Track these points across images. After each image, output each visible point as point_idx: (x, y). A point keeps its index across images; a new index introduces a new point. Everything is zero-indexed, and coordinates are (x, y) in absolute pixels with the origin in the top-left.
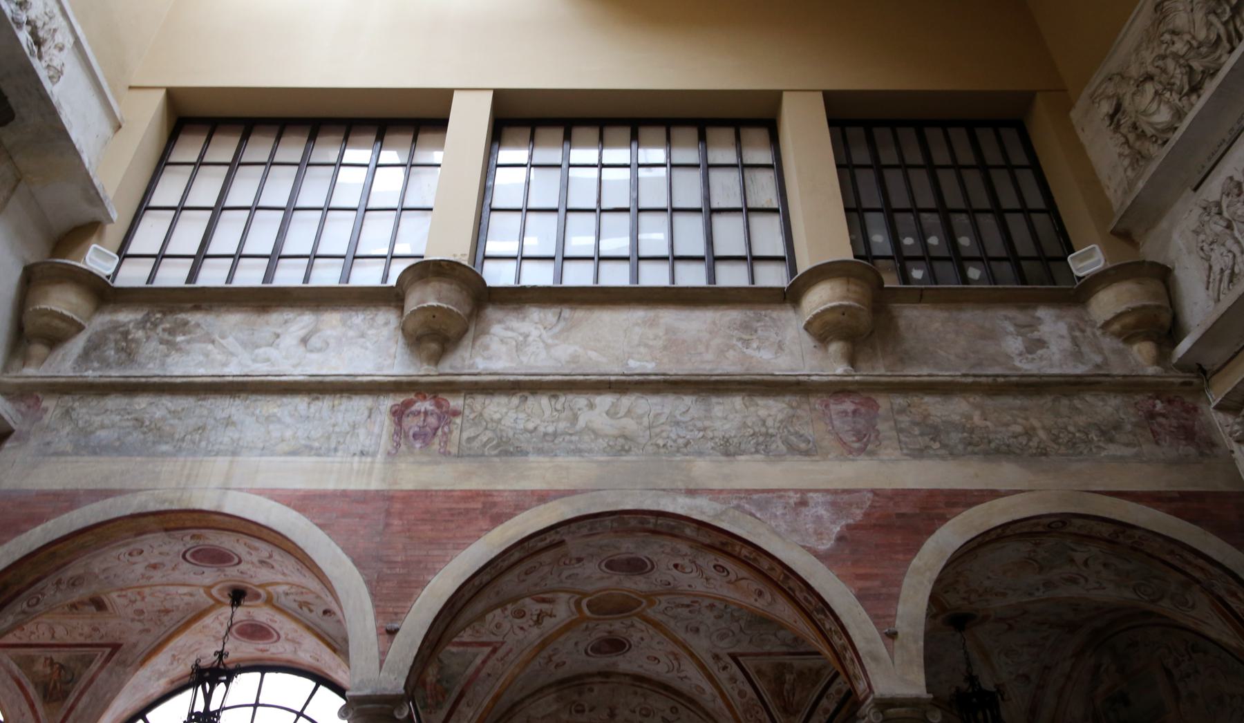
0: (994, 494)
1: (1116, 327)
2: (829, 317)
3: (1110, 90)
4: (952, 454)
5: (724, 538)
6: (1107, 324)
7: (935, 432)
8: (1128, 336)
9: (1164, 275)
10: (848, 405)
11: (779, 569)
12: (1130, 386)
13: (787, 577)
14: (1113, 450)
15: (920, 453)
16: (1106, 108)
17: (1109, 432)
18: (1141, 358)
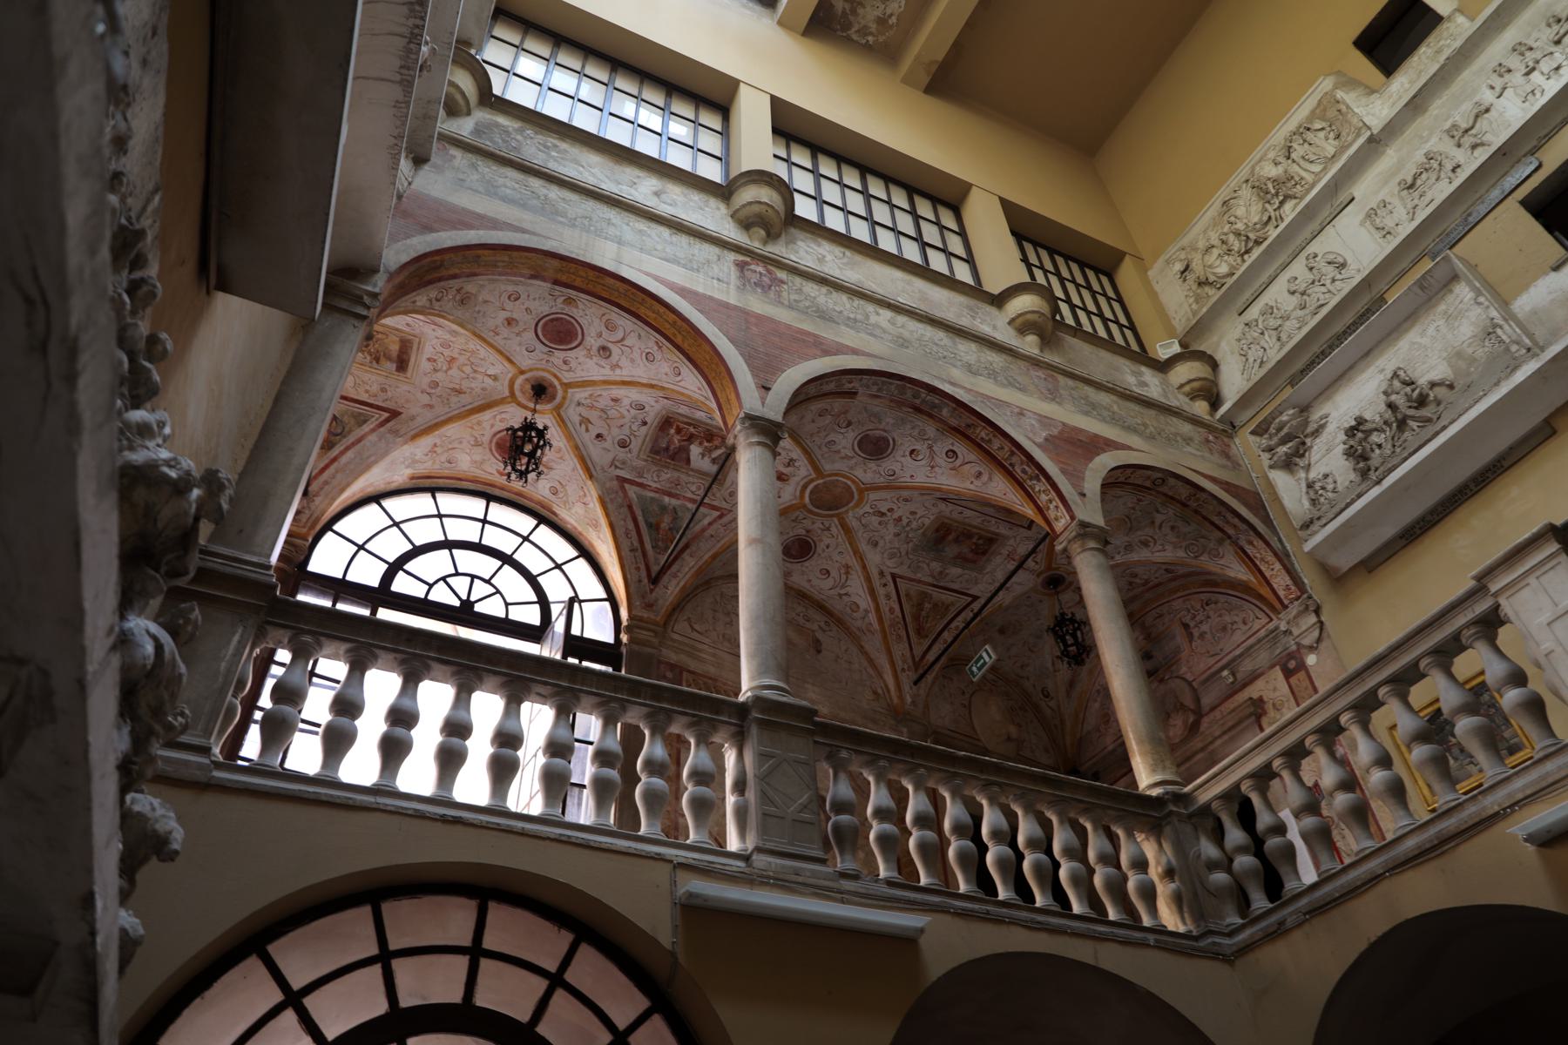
0: (1129, 448)
1: (1187, 388)
2: (1029, 317)
3: (1183, 256)
4: (1104, 420)
5: (969, 419)
6: (1182, 386)
7: (1094, 406)
8: (1193, 396)
9: (1214, 365)
10: (1040, 373)
11: (1008, 446)
12: (1195, 421)
13: (1013, 453)
14: (1189, 449)
15: (1086, 413)
16: (1179, 267)
17: (1188, 440)
18: (1200, 408)
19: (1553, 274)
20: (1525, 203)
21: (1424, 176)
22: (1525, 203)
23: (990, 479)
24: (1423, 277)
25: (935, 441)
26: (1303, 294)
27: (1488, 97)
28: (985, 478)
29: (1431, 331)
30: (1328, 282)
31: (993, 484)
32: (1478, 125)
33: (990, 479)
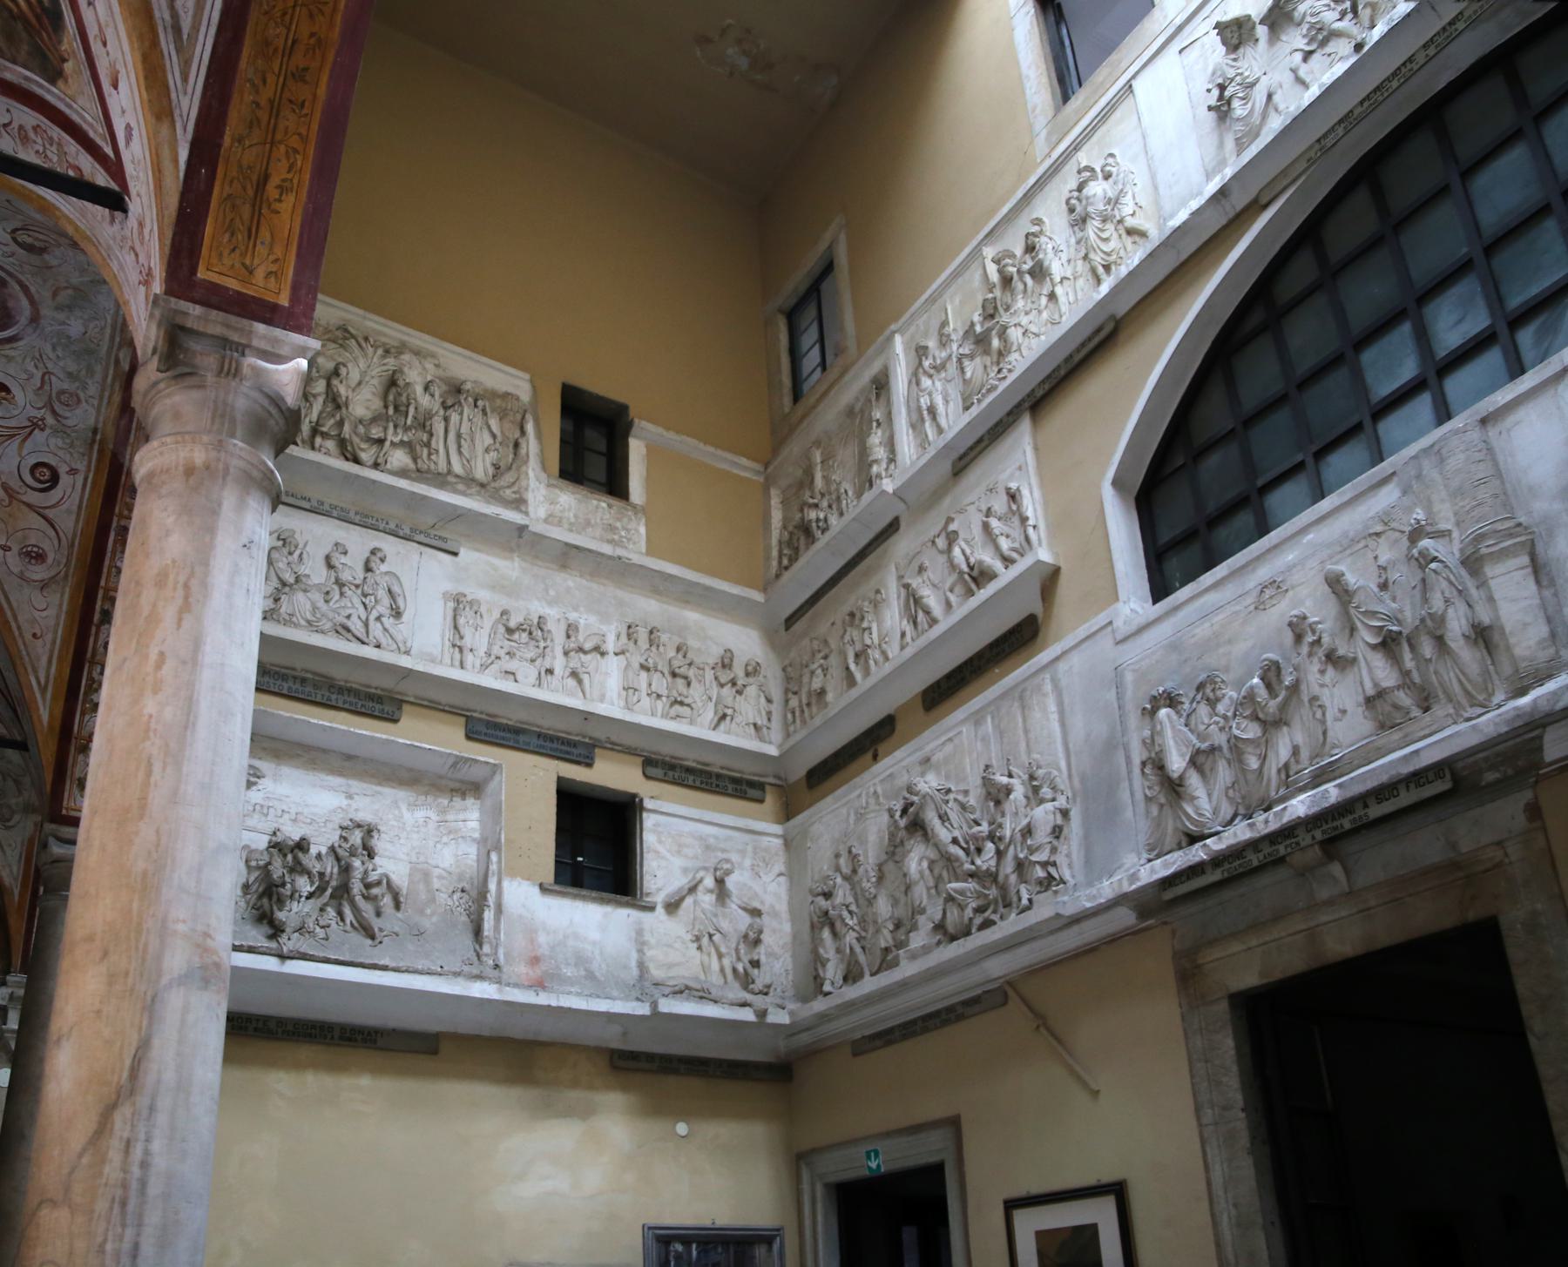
19: (536, 890)
20: (560, 780)
21: (525, 635)
22: (560, 780)
23: (44, 586)
24: (468, 760)
25: (61, 430)
26: (340, 584)
27: (610, 646)
28: (39, 572)
29: (420, 814)
30: (374, 614)
31: (39, 600)
32: (589, 657)
33: (44, 586)
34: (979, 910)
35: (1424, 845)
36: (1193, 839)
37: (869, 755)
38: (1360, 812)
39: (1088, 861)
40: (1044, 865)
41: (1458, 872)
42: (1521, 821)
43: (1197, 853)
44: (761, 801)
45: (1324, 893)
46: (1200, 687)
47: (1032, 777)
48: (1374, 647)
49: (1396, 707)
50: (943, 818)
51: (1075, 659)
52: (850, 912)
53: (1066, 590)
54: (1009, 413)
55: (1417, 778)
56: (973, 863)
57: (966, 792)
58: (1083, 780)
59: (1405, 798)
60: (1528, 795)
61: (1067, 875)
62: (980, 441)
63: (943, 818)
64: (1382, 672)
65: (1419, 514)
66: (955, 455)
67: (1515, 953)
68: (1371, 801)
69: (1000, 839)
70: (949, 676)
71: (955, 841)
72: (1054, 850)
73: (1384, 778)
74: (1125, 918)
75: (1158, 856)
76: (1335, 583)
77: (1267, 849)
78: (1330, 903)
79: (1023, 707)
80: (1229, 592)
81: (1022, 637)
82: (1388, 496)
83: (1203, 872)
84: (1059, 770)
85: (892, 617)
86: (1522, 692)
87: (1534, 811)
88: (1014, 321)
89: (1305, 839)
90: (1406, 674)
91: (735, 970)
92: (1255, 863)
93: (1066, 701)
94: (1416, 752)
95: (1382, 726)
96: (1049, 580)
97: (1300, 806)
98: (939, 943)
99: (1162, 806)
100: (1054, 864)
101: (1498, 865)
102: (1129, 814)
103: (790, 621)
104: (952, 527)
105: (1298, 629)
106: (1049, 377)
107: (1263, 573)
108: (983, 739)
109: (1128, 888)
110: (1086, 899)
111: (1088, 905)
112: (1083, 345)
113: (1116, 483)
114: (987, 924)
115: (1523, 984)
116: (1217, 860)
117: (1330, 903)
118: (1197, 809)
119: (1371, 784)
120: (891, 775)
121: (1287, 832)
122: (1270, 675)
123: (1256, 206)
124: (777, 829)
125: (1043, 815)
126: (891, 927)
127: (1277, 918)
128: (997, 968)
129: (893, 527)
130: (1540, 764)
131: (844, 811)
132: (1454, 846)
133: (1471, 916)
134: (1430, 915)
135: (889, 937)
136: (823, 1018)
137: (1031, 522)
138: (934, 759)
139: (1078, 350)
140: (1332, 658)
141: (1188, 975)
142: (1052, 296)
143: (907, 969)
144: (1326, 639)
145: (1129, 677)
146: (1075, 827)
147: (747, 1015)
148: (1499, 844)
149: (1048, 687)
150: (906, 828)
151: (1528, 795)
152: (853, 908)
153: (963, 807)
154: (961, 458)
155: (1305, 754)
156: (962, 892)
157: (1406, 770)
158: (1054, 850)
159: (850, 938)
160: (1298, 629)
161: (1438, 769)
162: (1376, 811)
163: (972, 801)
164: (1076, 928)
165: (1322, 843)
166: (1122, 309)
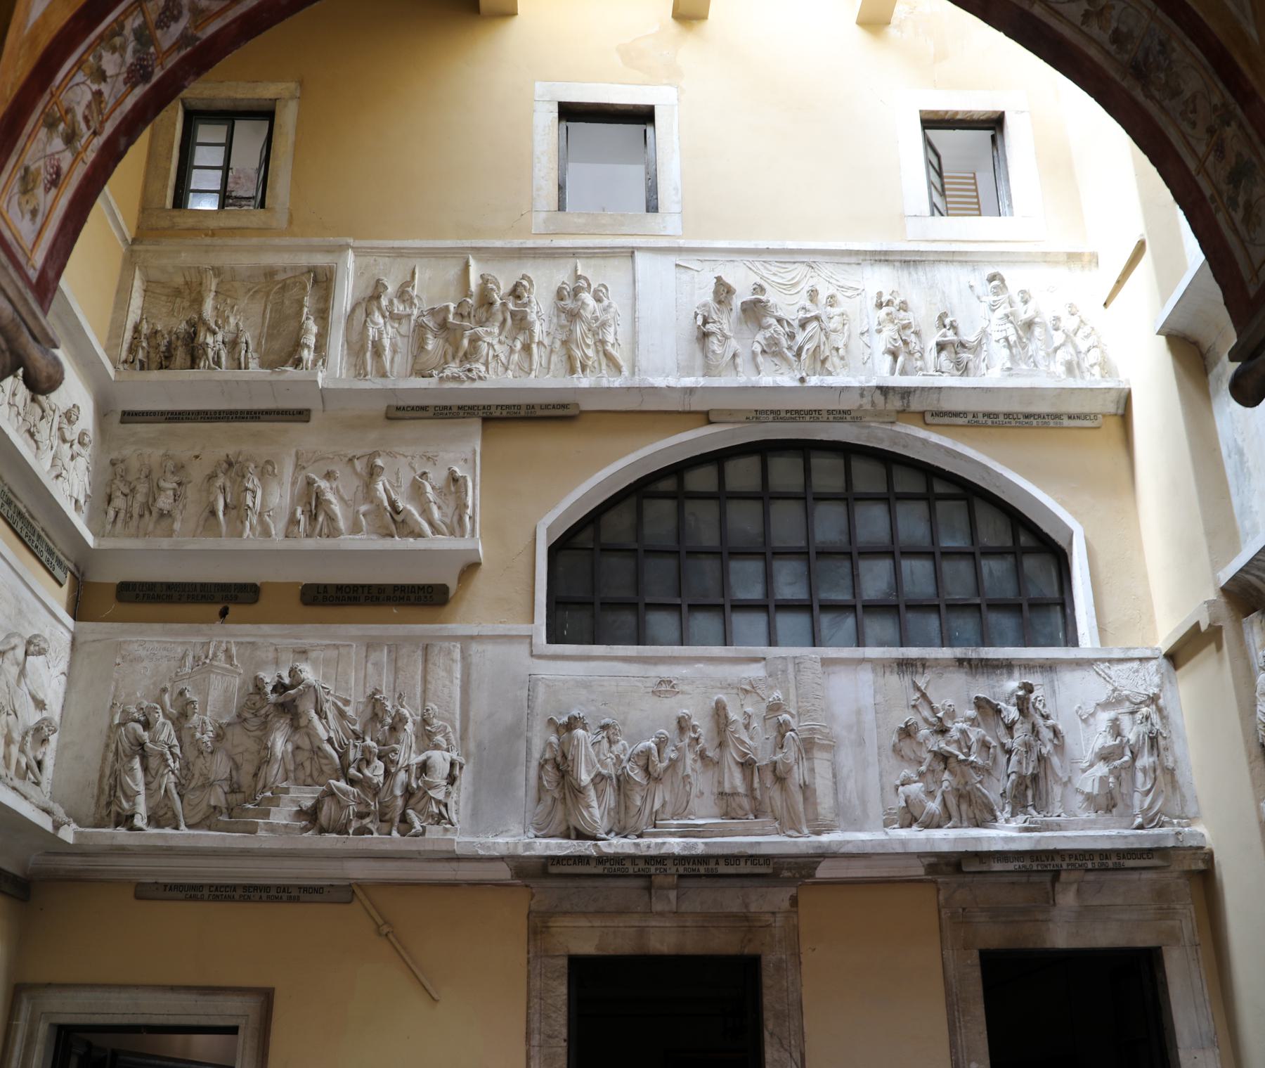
34: (361, 816)
35: (730, 900)
36: (581, 836)
37: (218, 608)
38: (712, 865)
39: (475, 813)
40: (438, 802)
41: (747, 922)
42: (786, 905)
43: (586, 848)
44: (61, 585)
45: (658, 906)
46: (605, 727)
47: (425, 722)
48: (738, 763)
49: (741, 807)
50: (321, 713)
51: (491, 650)
52: (172, 754)
53: (481, 583)
54: (460, 408)
55: (753, 859)
56: (359, 770)
57: (347, 702)
58: (479, 745)
59: (744, 868)
60: (793, 891)
61: (454, 819)
62: (424, 408)
63: (321, 713)
64: (736, 780)
65: (777, 694)
66: (394, 403)
67: (767, 981)
68: (722, 862)
69: (392, 761)
70: (339, 588)
71: (330, 740)
72: (448, 794)
73: (735, 851)
74: (503, 873)
75: (544, 837)
76: (719, 712)
77: (642, 865)
78: (661, 914)
79: (426, 661)
80: (634, 669)
81: (427, 598)
82: (756, 671)
83: (588, 863)
84: (453, 727)
85: (276, 498)
86: (818, 833)
87: (794, 901)
88: (488, 339)
89: (672, 870)
90: (751, 789)
91: (18, 762)
92: (631, 871)
93: (474, 676)
94: (759, 843)
95: (726, 815)
96: (471, 568)
97: (675, 845)
98: (305, 829)
99: (554, 800)
100: (446, 806)
101: (769, 926)
102: (522, 792)
103: (129, 417)
104: (379, 462)
105: (683, 725)
106: (508, 407)
107: (664, 671)
108: (375, 664)
109: (521, 851)
110: (462, 839)
111: (481, 852)
112: (547, 406)
113: (550, 530)
114: (363, 831)
115: (768, 999)
116: (602, 859)
117: (661, 914)
118: (591, 815)
119: (726, 851)
120: (253, 643)
121: (659, 859)
122: (661, 743)
123: (706, 418)
124: (69, 621)
125: (440, 761)
126: (227, 789)
127: (620, 912)
128: (358, 871)
129: (301, 415)
130: (812, 876)
131: (180, 650)
132: (747, 906)
133: (746, 951)
134: (722, 943)
135: (222, 797)
136: (122, 851)
137: (469, 511)
138: (313, 655)
139: (541, 407)
140: (702, 755)
141: (538, 928)
142: (527, 348)
143: (263, 839)
144: (702, 740)
145: (541, 690)
146: (465, 778)
147: (46, 823)
148: (773, 913)
149: (457, 655)
150: (276, 705)
151: (793, 891)
152: (177, 751)
153: (342, 714)
154: (398, 409)
155: (669, 809)
156: (345, 793)
157: (751, 852)
158: (448, 794)
159: (170, 780)
160: (683, 725)
161: (767, 858)
162: (723, 869)
163: (350, 711)
164: (454, 865)
165: (681, 876)
166: (585, 406)
